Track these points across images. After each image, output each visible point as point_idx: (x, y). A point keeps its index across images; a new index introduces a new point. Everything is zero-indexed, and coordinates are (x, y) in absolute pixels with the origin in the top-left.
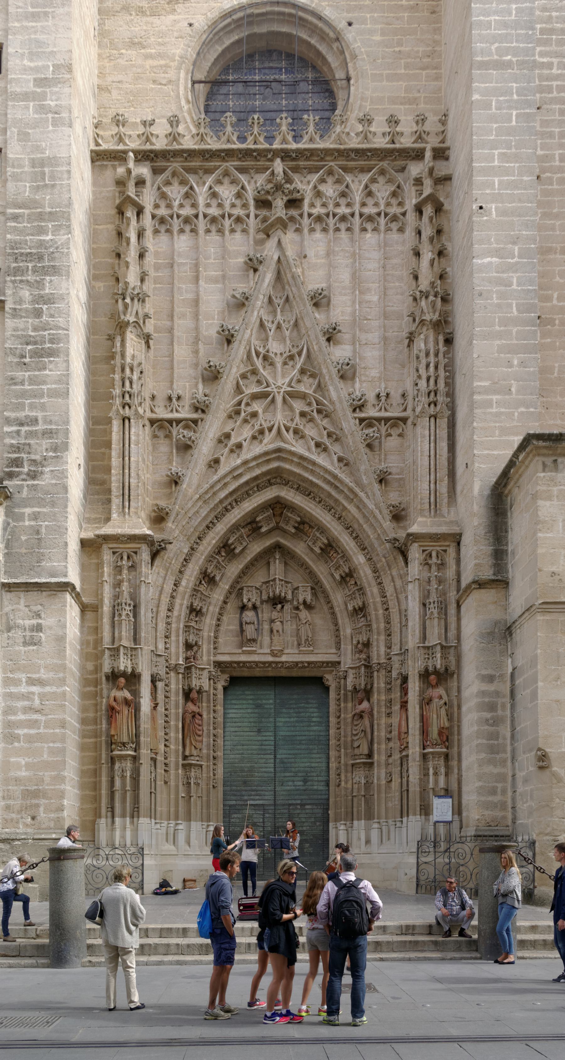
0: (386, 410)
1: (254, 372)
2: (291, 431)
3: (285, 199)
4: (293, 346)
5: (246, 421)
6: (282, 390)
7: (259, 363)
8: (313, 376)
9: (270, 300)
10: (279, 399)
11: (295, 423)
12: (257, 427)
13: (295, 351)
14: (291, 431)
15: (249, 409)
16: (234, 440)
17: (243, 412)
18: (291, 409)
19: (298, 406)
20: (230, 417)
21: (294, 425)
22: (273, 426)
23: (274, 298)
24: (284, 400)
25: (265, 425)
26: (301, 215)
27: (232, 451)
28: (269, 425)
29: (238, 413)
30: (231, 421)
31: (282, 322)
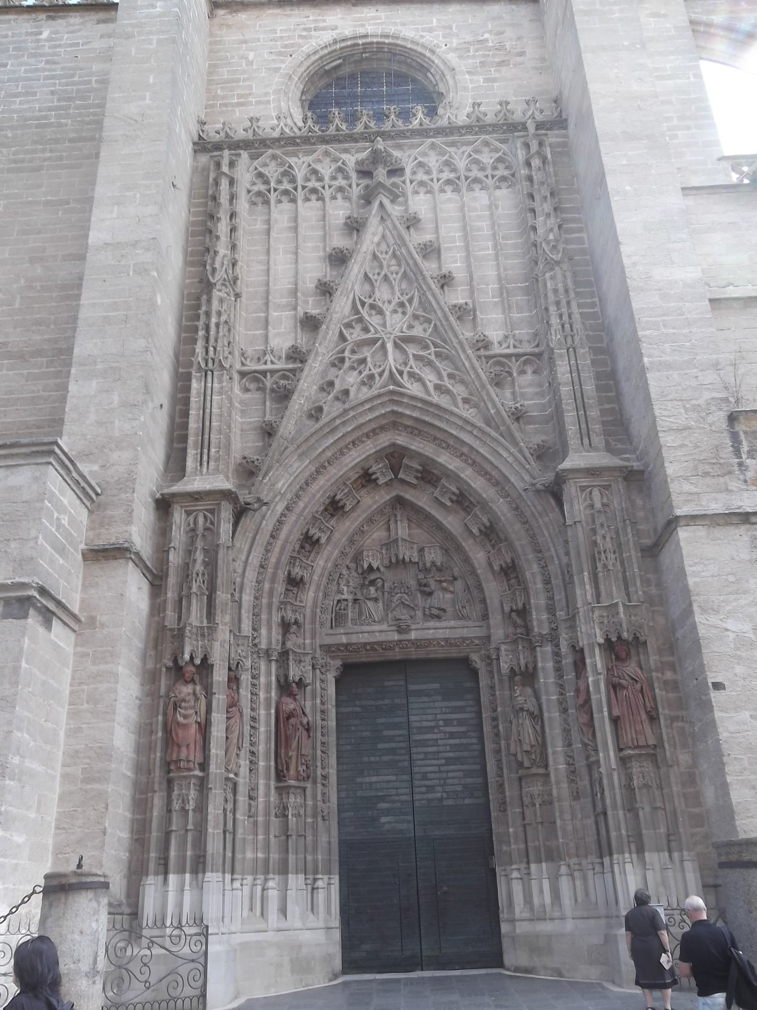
0: (515, 347)
1: (361, 320)
2: (405, 376)
3: (387, 169)
4: (402, 294)
5: (353, 368)
6: (392, 336)
7: (364, 312)
8: (429, 321)
9: (375, 257)
10: (390, 346)
11: (409, 366)
12: (364, 374)
13: (405, 298)
14: (405, 376)
15: (355, 357)
16: (338, 386)
17: (347, 359)
18: (403, 351)
19: (412, 350)
20: (333, 365)
21: (408, 369)
22: (383, 371)
23: (378, 254)
24: (396, 345)
25: (375, 371)
26: (404, 182)
27: (337, 399)
28: (379, 370)
29: (342, 360)
30: (333, 370)
31: (389, 274)
